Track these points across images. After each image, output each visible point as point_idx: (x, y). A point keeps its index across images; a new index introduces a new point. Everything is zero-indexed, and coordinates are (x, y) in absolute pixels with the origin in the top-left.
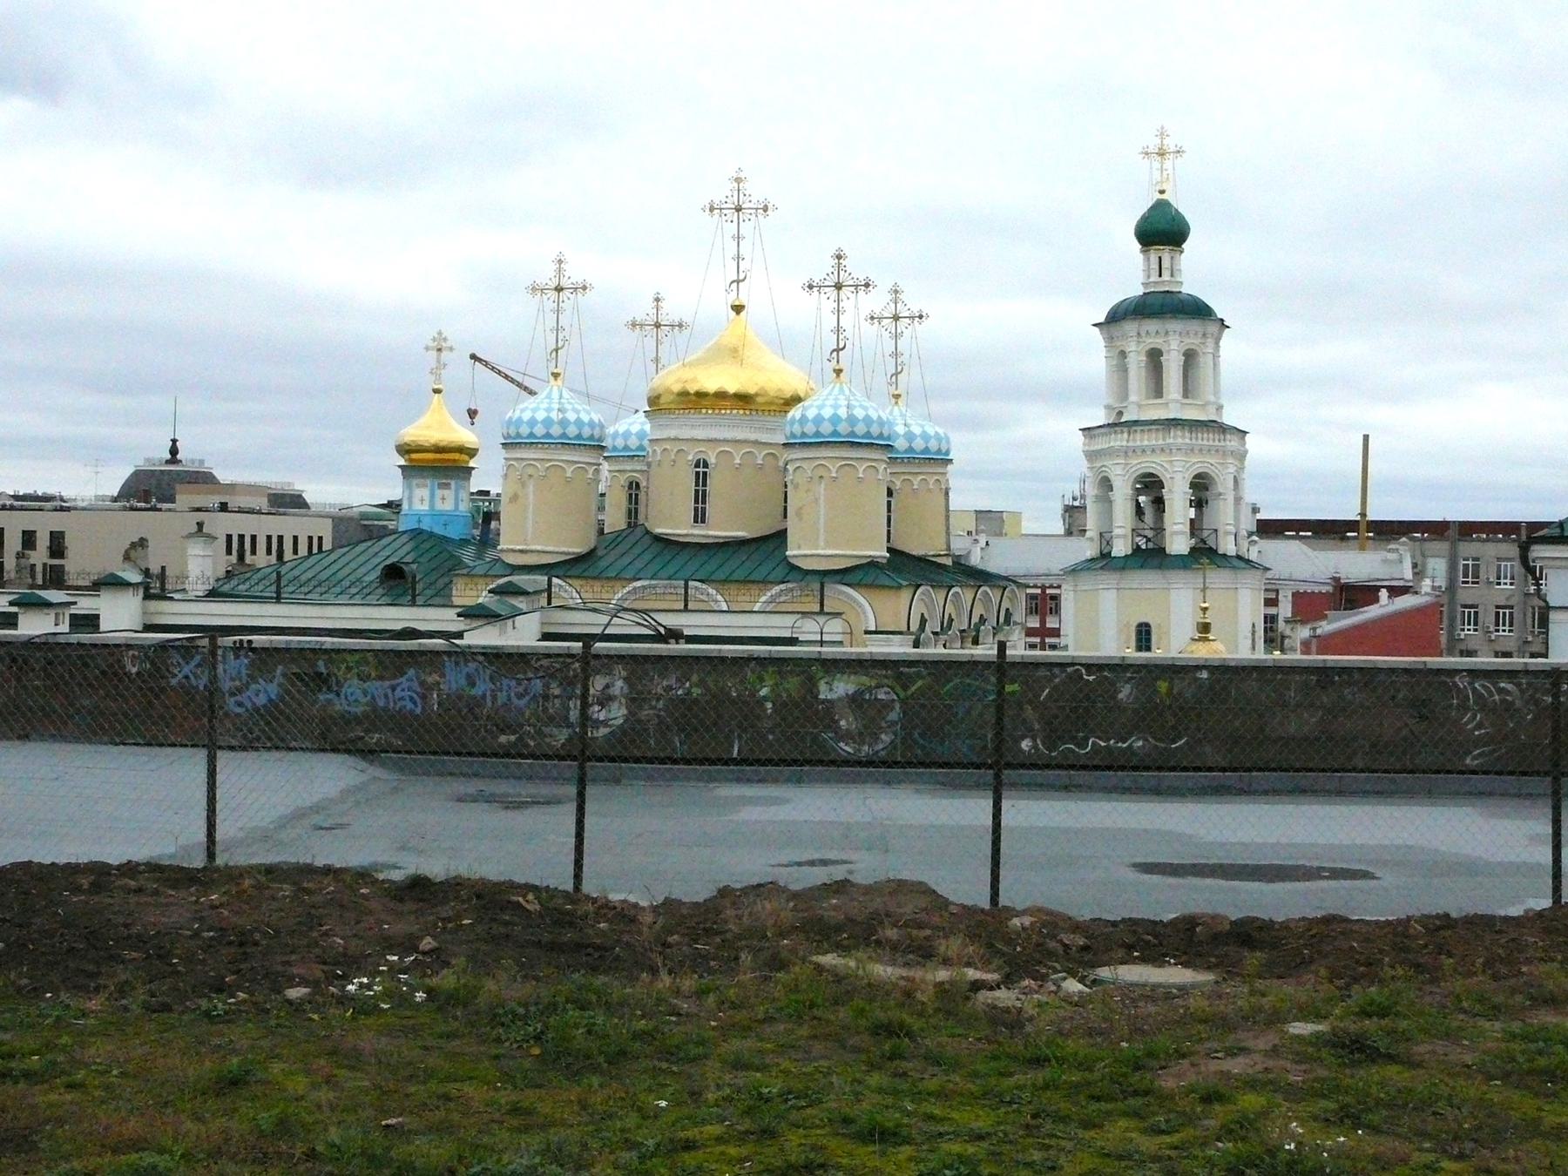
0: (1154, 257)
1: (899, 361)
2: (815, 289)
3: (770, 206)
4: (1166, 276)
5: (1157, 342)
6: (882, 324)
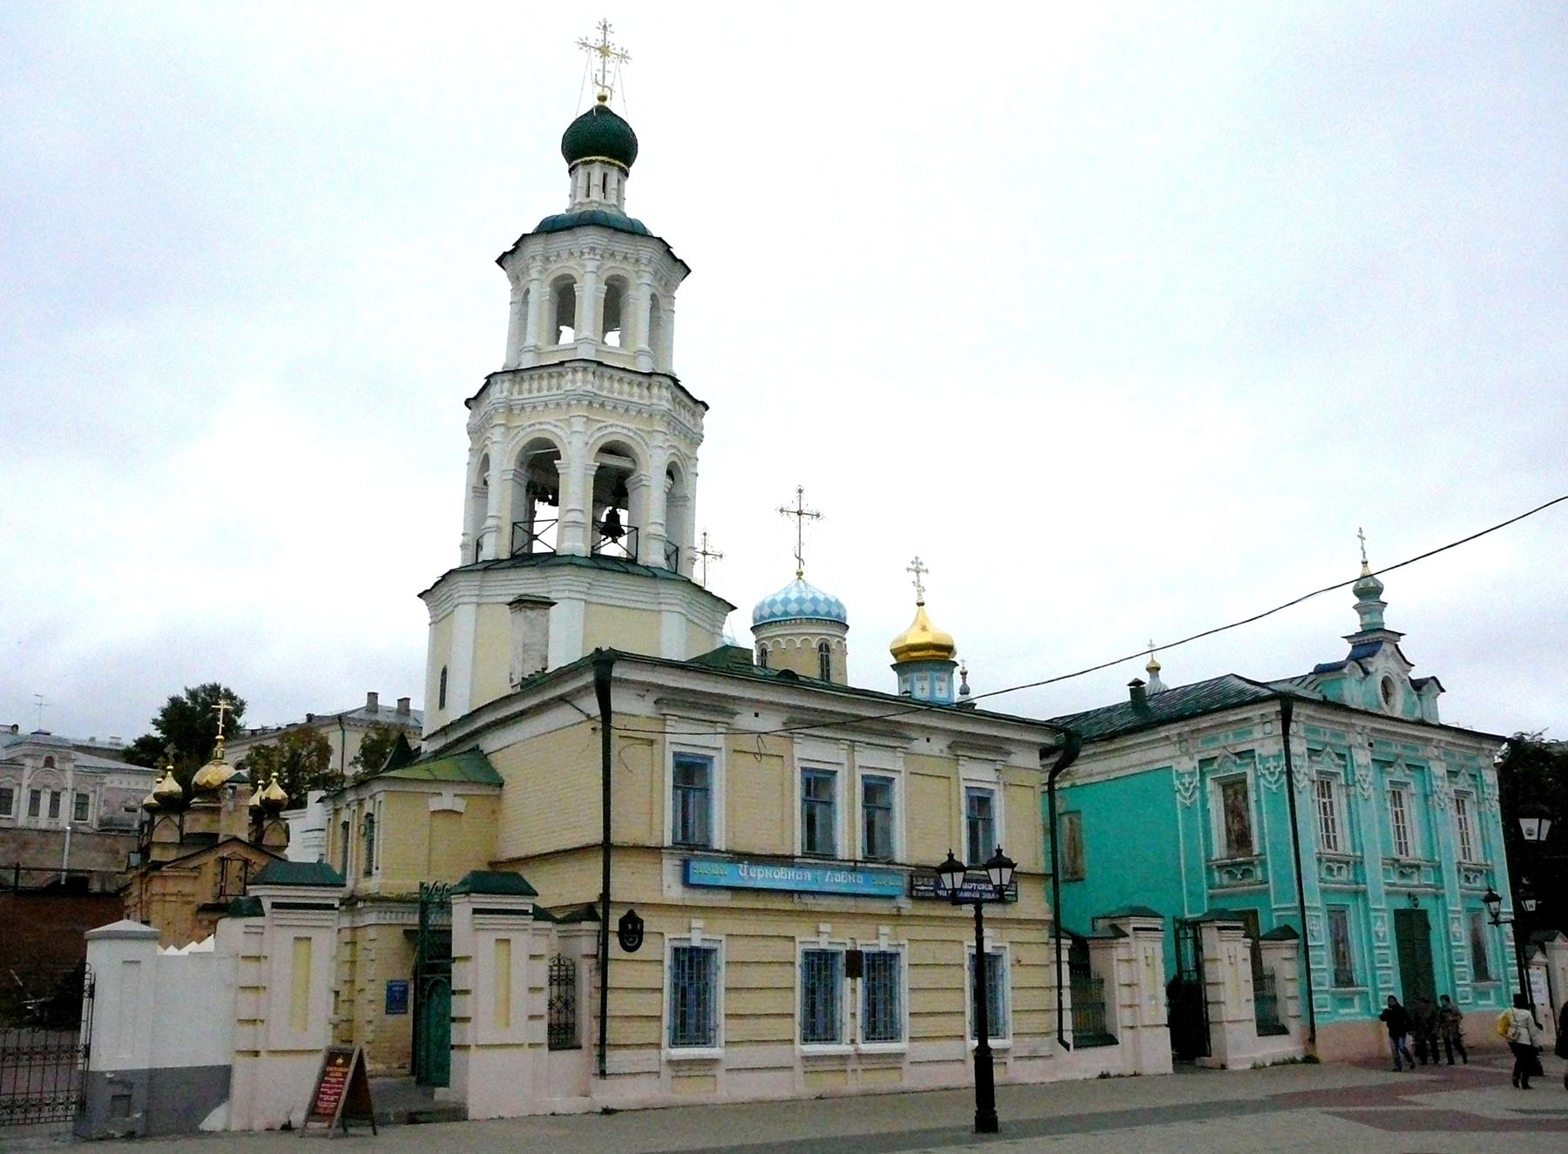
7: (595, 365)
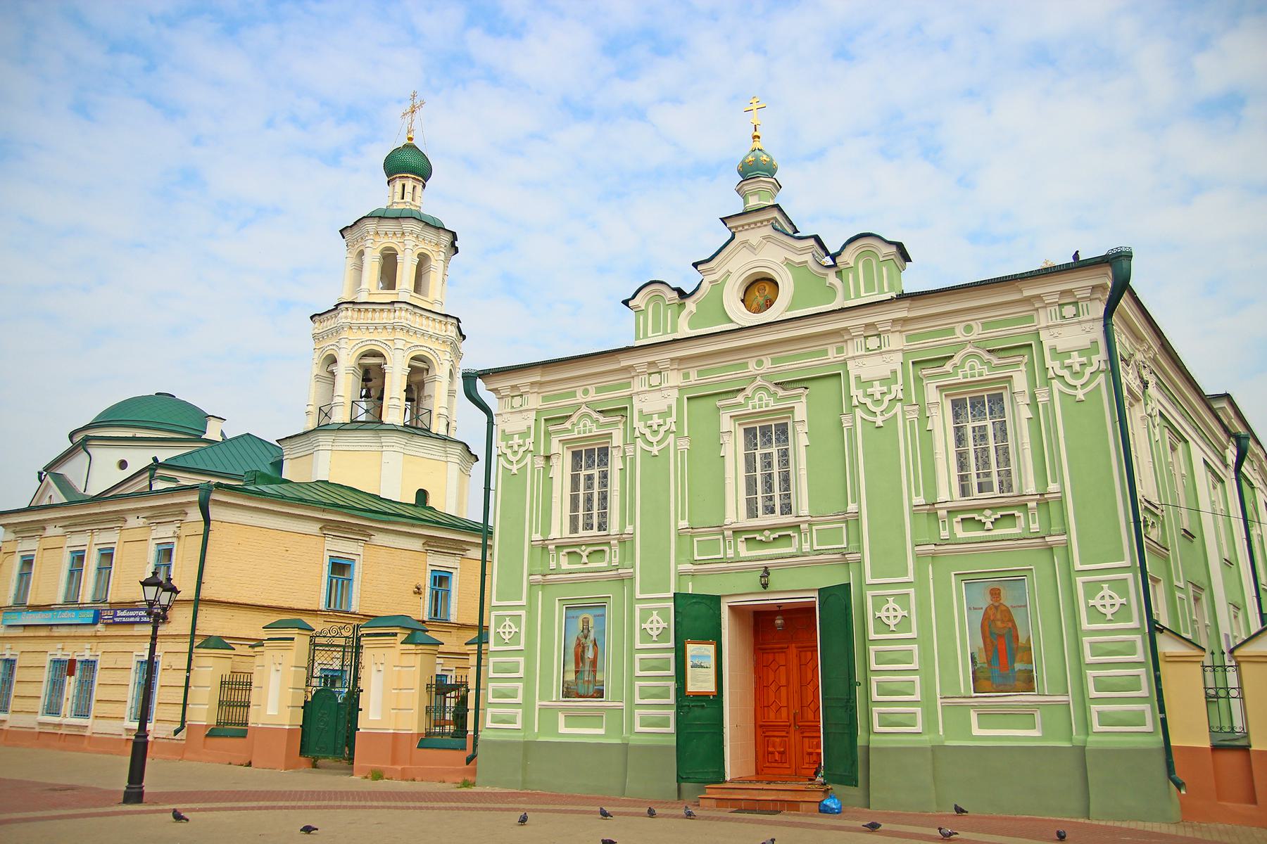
4: (408, 197)
7: (317, 317)
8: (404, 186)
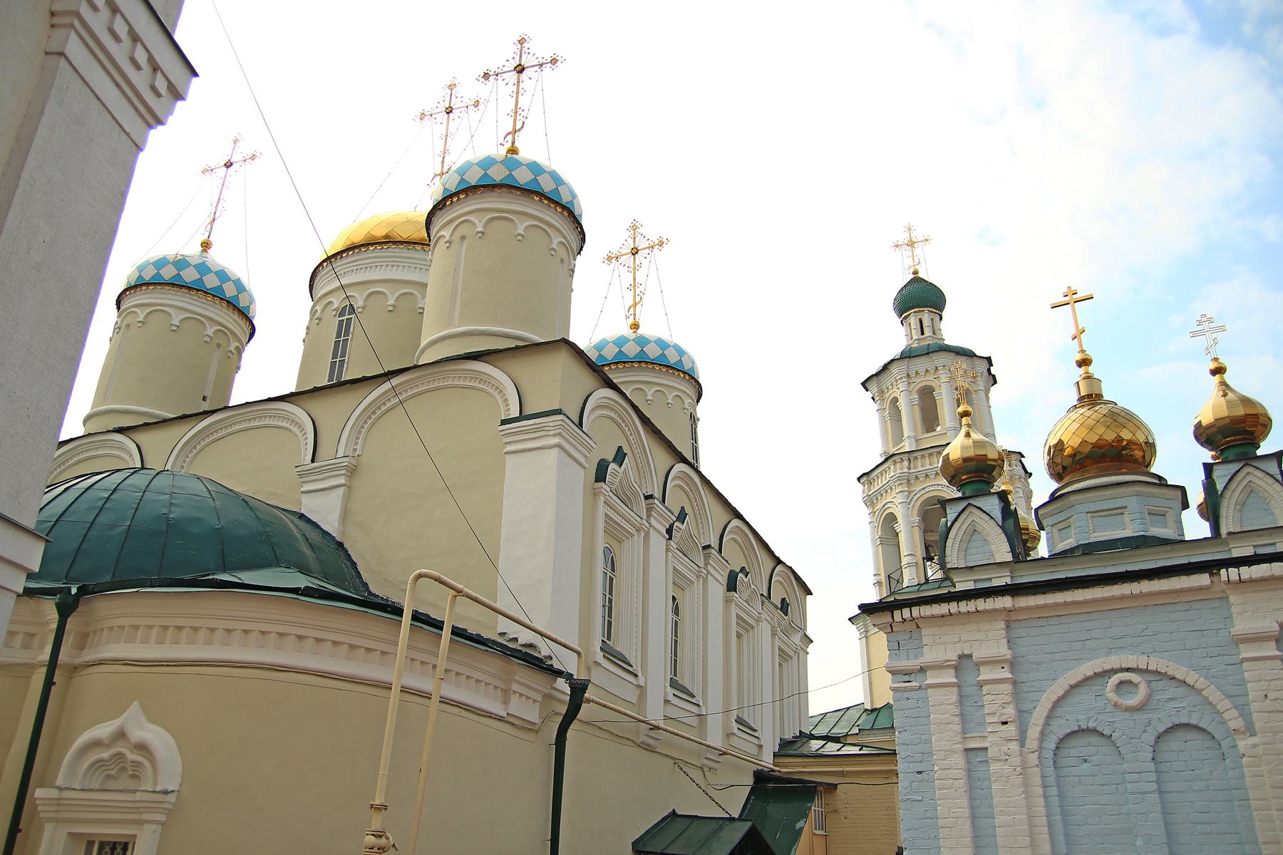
0: (913, 320)
1: (638, 292)
2: (492, 78)
3: (481, 101)
4: (928, 332)
5: (928, 380)
6: (620, 262)
8: (921, 321)
